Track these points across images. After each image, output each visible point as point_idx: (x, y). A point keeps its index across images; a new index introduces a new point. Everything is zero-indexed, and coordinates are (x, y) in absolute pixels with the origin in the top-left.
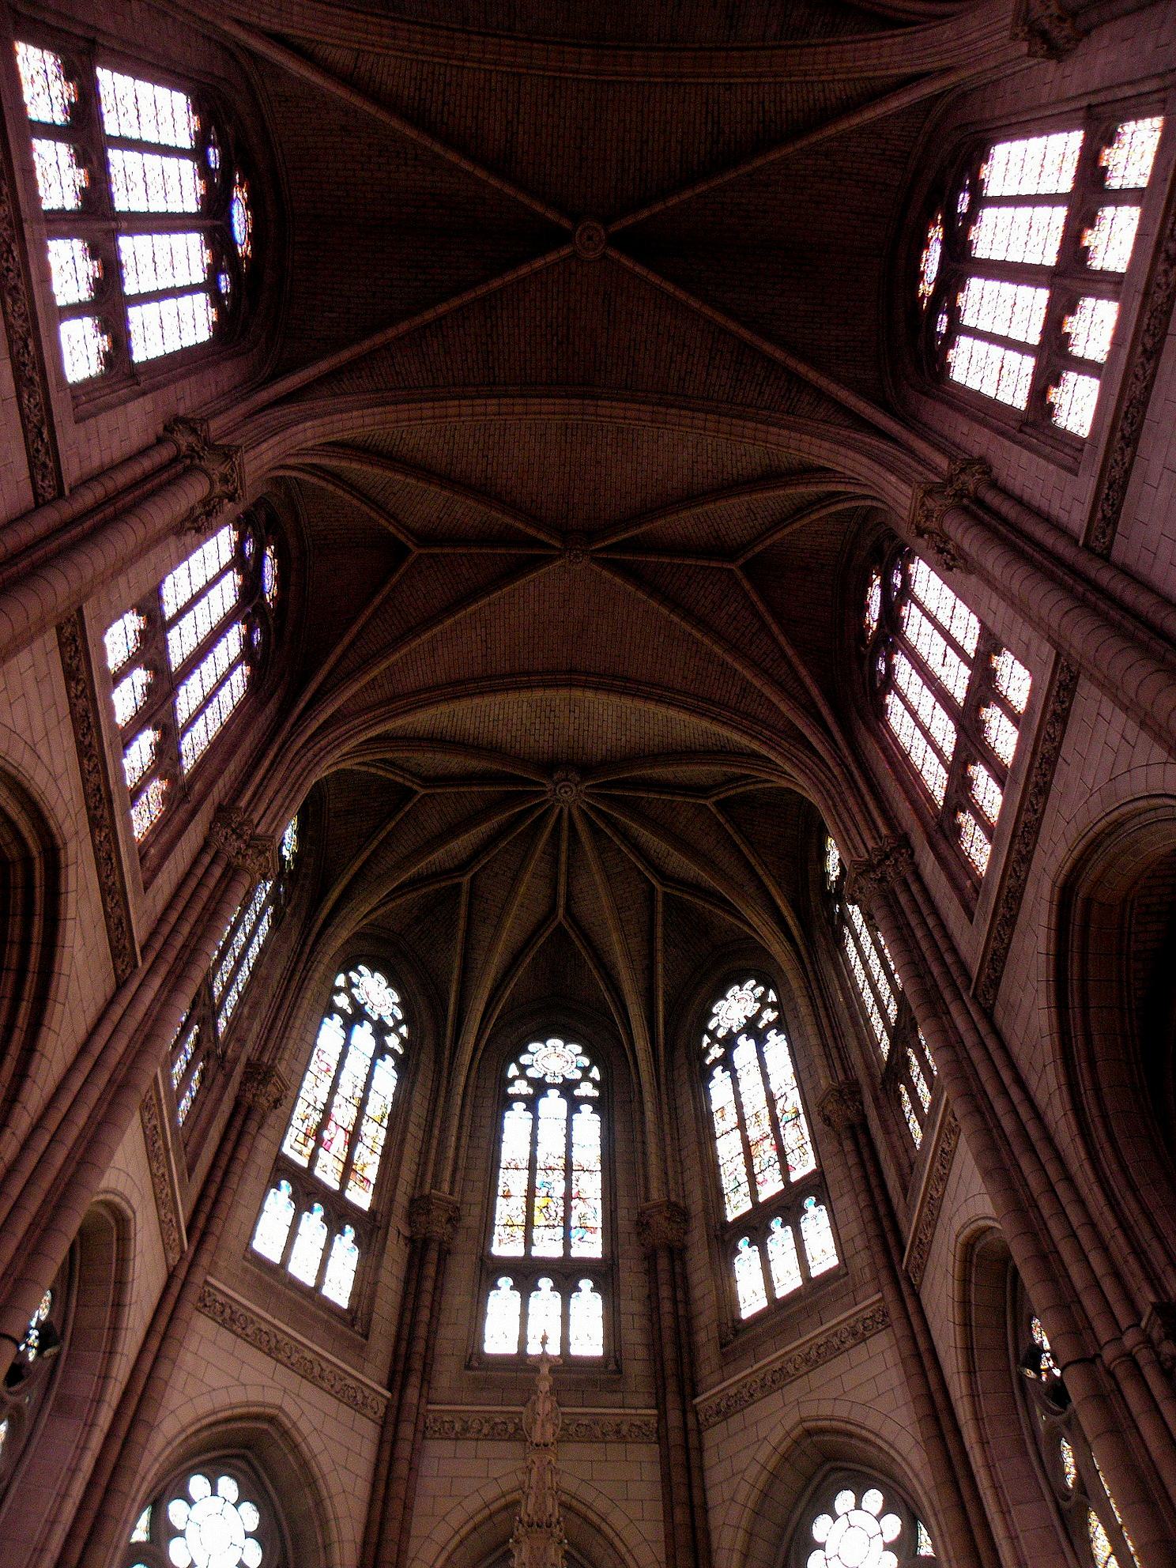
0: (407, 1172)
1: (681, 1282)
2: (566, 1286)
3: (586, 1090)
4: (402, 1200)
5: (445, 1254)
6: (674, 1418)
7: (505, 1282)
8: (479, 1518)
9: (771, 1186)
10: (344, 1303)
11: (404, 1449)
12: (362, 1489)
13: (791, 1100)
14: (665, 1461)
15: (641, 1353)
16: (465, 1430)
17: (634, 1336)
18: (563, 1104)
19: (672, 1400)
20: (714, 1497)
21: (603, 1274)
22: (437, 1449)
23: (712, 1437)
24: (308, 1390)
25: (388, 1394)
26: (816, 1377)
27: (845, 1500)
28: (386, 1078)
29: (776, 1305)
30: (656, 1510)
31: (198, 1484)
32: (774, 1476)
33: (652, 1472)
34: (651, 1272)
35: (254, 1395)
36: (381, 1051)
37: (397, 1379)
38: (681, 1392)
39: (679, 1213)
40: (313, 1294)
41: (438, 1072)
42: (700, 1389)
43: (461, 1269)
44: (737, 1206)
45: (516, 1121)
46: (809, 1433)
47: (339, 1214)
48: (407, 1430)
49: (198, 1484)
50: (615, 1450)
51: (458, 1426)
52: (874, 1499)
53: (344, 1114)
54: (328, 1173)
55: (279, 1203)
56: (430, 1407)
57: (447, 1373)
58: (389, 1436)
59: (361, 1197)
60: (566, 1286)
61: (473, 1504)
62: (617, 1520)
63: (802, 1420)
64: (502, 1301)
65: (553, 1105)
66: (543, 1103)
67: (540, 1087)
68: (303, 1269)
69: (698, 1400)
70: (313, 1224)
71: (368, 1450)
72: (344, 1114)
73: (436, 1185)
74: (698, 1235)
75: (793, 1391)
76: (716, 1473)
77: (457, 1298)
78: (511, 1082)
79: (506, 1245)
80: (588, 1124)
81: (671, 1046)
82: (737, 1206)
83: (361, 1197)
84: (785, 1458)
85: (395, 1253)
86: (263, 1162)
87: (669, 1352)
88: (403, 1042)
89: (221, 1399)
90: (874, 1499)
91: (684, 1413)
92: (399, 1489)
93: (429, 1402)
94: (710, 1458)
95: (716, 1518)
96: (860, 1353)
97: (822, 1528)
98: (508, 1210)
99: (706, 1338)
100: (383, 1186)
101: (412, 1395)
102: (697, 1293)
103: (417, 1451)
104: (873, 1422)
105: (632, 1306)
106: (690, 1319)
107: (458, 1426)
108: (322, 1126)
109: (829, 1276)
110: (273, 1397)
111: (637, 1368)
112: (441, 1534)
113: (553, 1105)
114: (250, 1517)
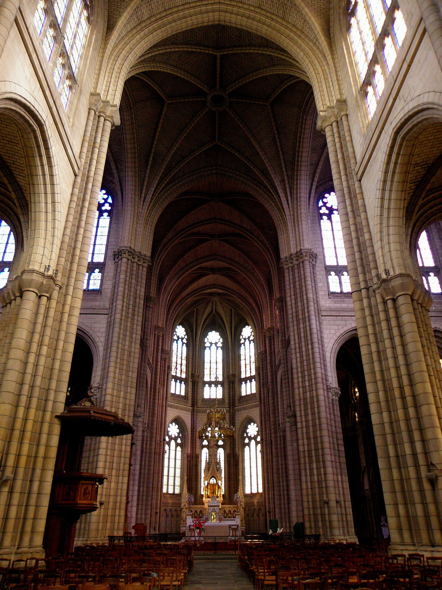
0: (190, 369)
1: (234, 388)
2: (216, 386)
3: (220, 345)
4: (190, 374)
5: (198, 382)
6: (231, 410)
7: (207, 385)
9: (248, 375)
10: (184, 395)
12: (190, 421)
13: (253, 359)
15: (227, 399)
17: (226, 396)
18: (216, 347)
19: (231, 408)
20: (236, 421)
21: (222, 384)
23: (237, 413)
24: (182, 411)
27: (252, 424)
28: (185, 347)
29: (247, 396)
31: (170, 425)
34: (229, 385)
35: (176, 415)
36: (183, 343)
37: (193, 405)
39: (234, 375)
40: (179, 396)
41: (193, 343)
43: (200, 384)
44: (243, 376)
45: (207, 351)
47: (181, 380)
48: (195, 413)
49: (170, 425)
52: (256, 425)
53: (179, 362)
54: (179, 375)
55: (173, 382)
57: (200, 403)
59: (184, 376)
60: (216, 386)
64: (207, 388)
65: (213, 347)
66: (211, 347)
67: (211, 344)
68: (178, 393)
70: (178, 384)
71: (190, 416)
72: (179, 362)
73: (195, 372)
74: (237, 380)
75: (247, 411)
76: (236, 419)
77: (200, 390)
78: (205, 343)
79: (207, 379)
80: (220, 351)
81: (235, 338)
82: (243, 376)
83: (184, 376)
85: (190, 384)
86: (170, 377)
87: (231, 400)
88: (187, 340)
89: (172, 417)
90: (256, 425)
96: (255, 409)
97: (249, 426)
98: (207, 372)
99: (237, 398)
100: (187, 373)
101: (195, 408)
102: (236, 390)
105: (226, 391)
106: (235, 394)
108: (176, 366)
109: (254, 394)
110: (178, 414)
111: (227, 401)
113: (213, 347)
114: (177, 426)
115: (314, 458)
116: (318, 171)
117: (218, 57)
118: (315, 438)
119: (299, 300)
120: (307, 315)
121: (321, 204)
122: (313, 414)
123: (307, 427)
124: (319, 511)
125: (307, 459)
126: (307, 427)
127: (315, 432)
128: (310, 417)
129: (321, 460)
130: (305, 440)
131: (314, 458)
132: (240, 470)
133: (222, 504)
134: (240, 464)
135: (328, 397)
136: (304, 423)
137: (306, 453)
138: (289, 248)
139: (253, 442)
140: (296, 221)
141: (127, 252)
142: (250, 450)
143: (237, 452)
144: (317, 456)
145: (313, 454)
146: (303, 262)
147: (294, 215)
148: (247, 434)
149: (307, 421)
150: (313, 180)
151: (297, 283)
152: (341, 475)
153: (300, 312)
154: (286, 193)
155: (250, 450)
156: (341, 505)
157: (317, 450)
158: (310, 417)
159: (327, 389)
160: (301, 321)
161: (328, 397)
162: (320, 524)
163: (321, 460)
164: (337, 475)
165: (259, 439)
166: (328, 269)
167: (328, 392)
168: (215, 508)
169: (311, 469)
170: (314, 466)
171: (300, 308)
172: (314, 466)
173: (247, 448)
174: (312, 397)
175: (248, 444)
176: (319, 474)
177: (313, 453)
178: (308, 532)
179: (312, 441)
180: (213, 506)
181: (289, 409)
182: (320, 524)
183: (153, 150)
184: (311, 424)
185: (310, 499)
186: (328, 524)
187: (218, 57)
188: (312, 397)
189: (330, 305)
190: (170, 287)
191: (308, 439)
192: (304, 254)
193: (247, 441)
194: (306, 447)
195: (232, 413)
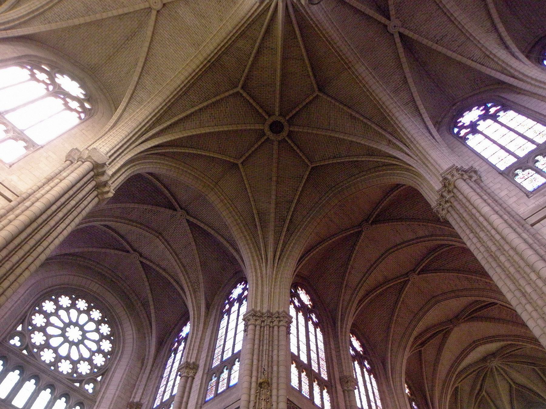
116: (419, 102)
117: (241, 91)
119: (478, 230)
120: (498, 237)
121: (456, 130)
138: (432, 189)
140: (425, 160)
141: (251, 317)
146: (455, 187)
147: (420, 159)
150: (421, 115)
151: (465, 215)
153: (490, 244)
154: (401, 150)
160: (498, 254)
166: (506, 173)
171: (485, 239)
183: (255, 212)
187: (241, 91)
189: (537, 203)
190: (398, 365)
192: (449, 177)
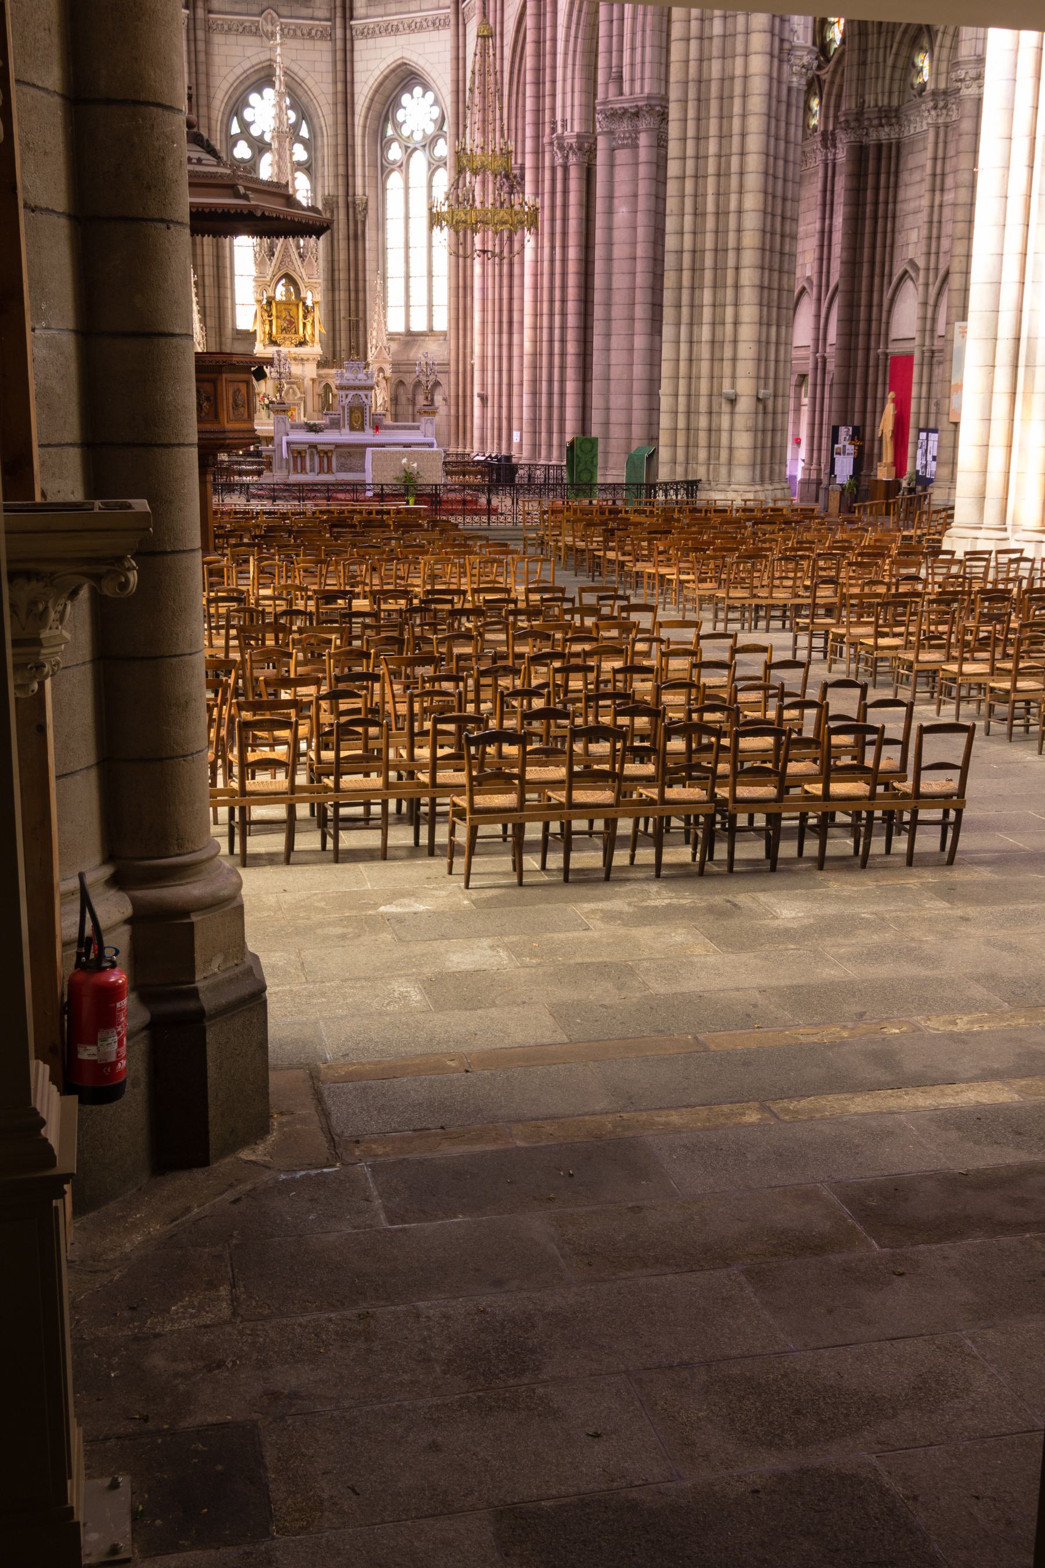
6: (339, 32)
8: (241, 78)
11: (201, 46)
14: (335, 52)
16: (230, 29)
22: (218, 39)
23: (359, 44)
25: (187, 12)
26: (414, 38)
27: (418, 91)
30: (329, 77)
32: (386, 77)
33: (328, 57)
38: (344, 17)
42: (356, 13)
46: (406, 64)
48: (200, 34)
50: (309, 44)
51: (226, 27)
56: (212, 16)
58: (192, 37)
61: (238, 71)
62: (309, 82)
63: (402, 58)
69: (353, 23)
75: (401, 39)
76: (358, 66)
84: (393, 71)
91: (345, 29)
92: (202, 68)
93: (210, 12)
94: (357, 56)
95: (357, 88)
96: (435, 34)
97: (405, 99)
101: (200, 13)
103: (208, 42)
104: (434, 75)
107: (226, 27)
112: (225, 86)
115: (708, 275)
118: (721, 214)
122: (723, 137)
123: (699, 177)
124: (703, 422)
125: (686, 275)
126: (699, 177)
127: (721, 194)
128: (712, 147)
129: (730, 281)
130: (688, 219)
131: (708, 275)
132: (370, 255)
133: (320, 365)
134: (370, 234)
135: (779, 82)
136: (690, 164)
137: (687, 258)
139: (419, 162)
142: (407, 188)
143: (359, 190)
144: (718, 268)
145: (709, 261)
148: (397, 126)
149: (700, 157)
152: (778, 326)
155: (407, 188)
156: (765, 408)
157: (719, 251)
158: (712, 147)
159: (781, 49)
161: (779, 82)
162: (702, 454)
163: (730, 281)
164: (769, 325)
165: (442, 149)
167: (781, 61)
168: (362, 393)
169: (695, 307)
170: (707, 296)
172: (707, 296)
173: (395, 181)
174: (726, 79)
175: (403, 167)
176: (716, 323)
177: (709, 261)
178: (664, 474)
179: (710, 223)
180: (355, 388)
181: (612, 89)
182: (702, 454)
184: (711, 168)
185: (682, 389)
186: (724, 455)
188: (726, 79)
191: (698, 214)
193: (395, 153)
194: (688, 239)
195: (339, 44)
